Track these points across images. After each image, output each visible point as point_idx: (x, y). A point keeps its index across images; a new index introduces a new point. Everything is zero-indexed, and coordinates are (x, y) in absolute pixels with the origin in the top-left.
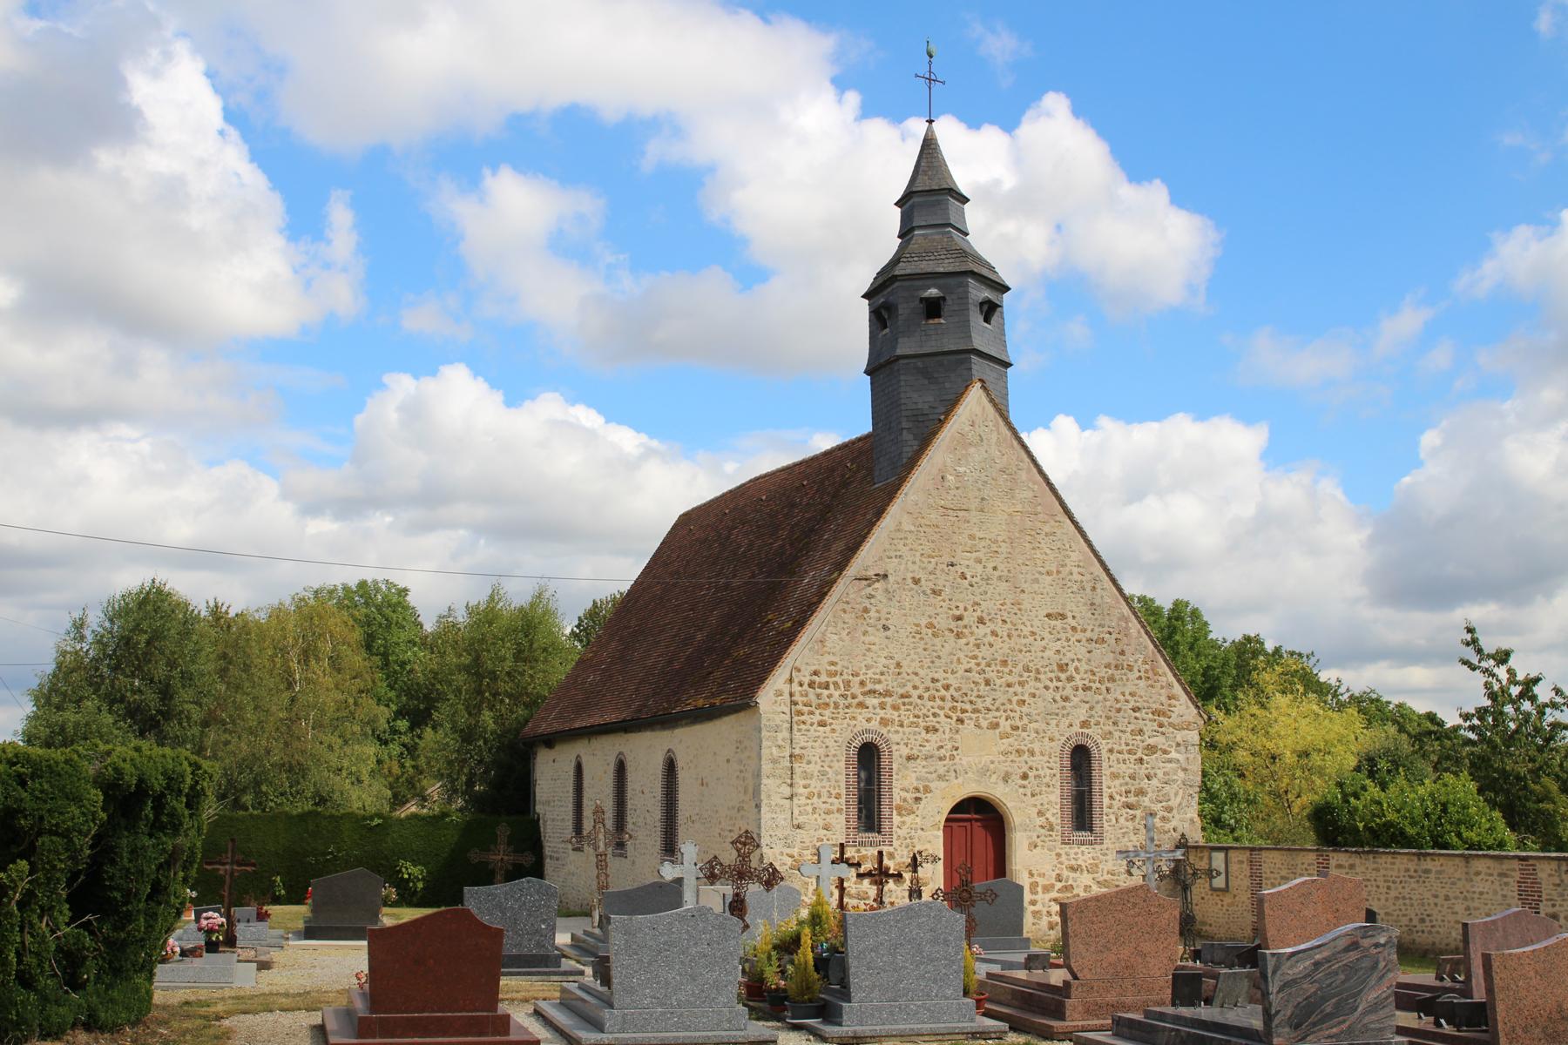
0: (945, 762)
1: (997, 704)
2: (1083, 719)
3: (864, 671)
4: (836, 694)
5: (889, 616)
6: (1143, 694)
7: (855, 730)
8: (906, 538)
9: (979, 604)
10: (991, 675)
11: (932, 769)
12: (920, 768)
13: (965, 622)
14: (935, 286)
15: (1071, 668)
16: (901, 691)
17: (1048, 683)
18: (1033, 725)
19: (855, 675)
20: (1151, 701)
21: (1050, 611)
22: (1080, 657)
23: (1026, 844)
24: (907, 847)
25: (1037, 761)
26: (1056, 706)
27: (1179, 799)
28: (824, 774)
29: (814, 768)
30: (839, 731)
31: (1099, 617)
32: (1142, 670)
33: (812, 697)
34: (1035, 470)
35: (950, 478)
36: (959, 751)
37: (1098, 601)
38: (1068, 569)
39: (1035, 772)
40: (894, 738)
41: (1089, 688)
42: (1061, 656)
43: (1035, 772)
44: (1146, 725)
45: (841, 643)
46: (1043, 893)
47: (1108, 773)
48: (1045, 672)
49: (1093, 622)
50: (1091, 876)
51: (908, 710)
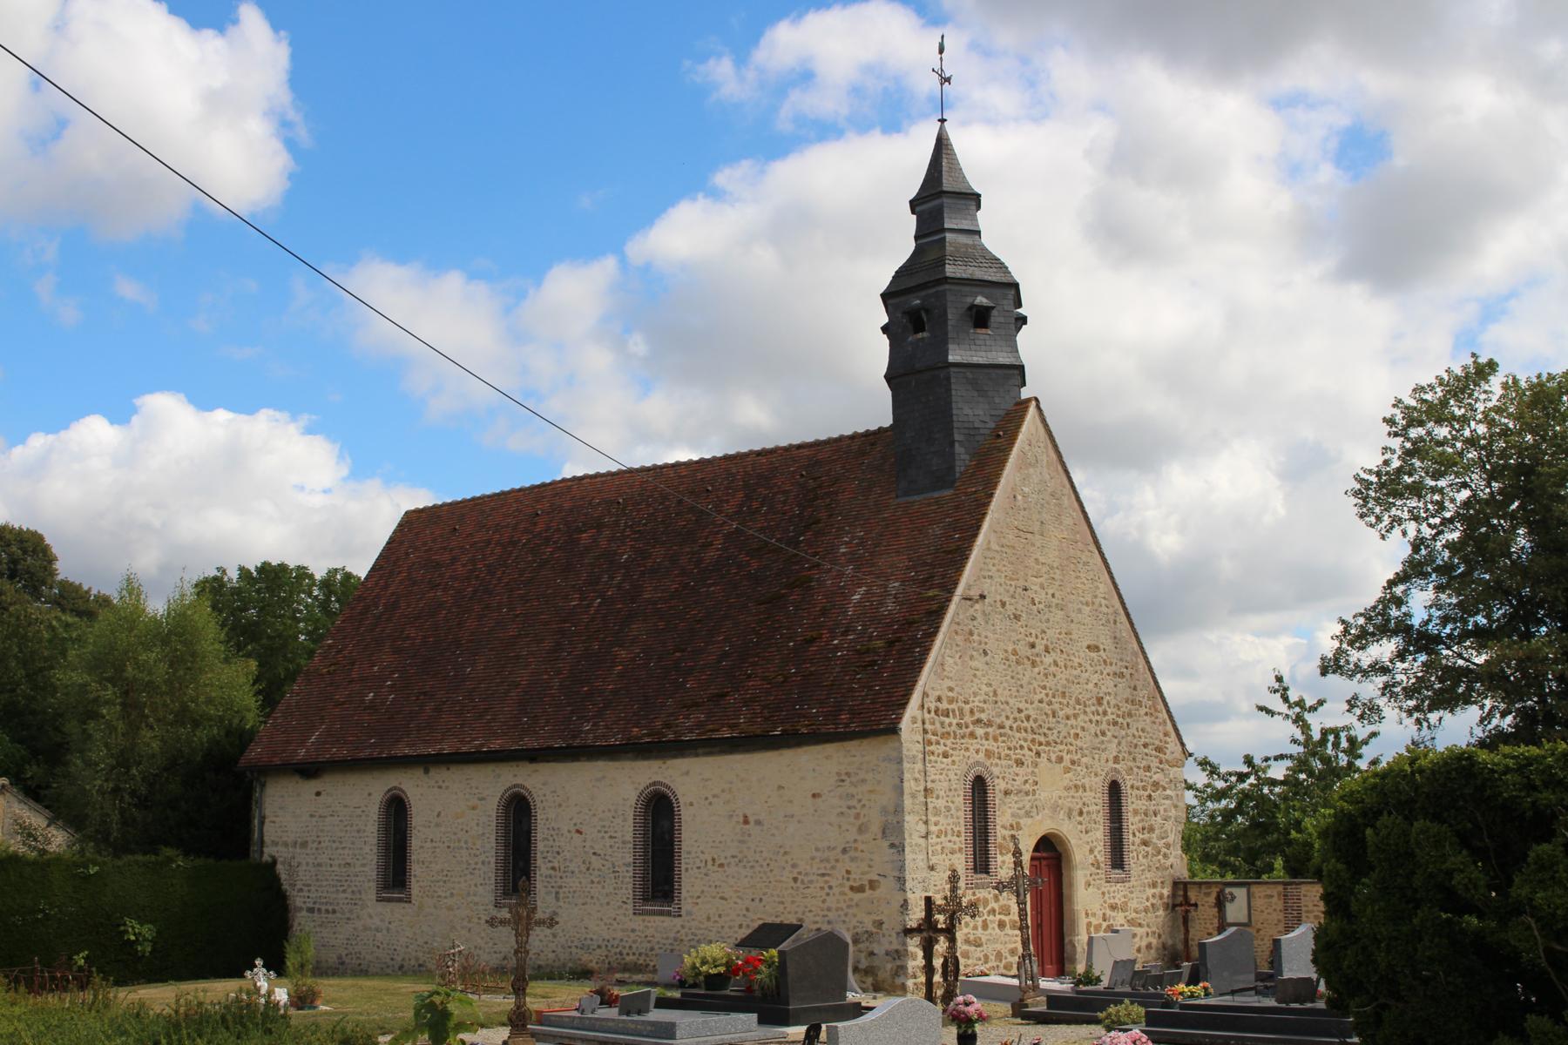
18: (1084, 760)
19: (966, 702)
34: (1073, 496)
40: (996, 771)
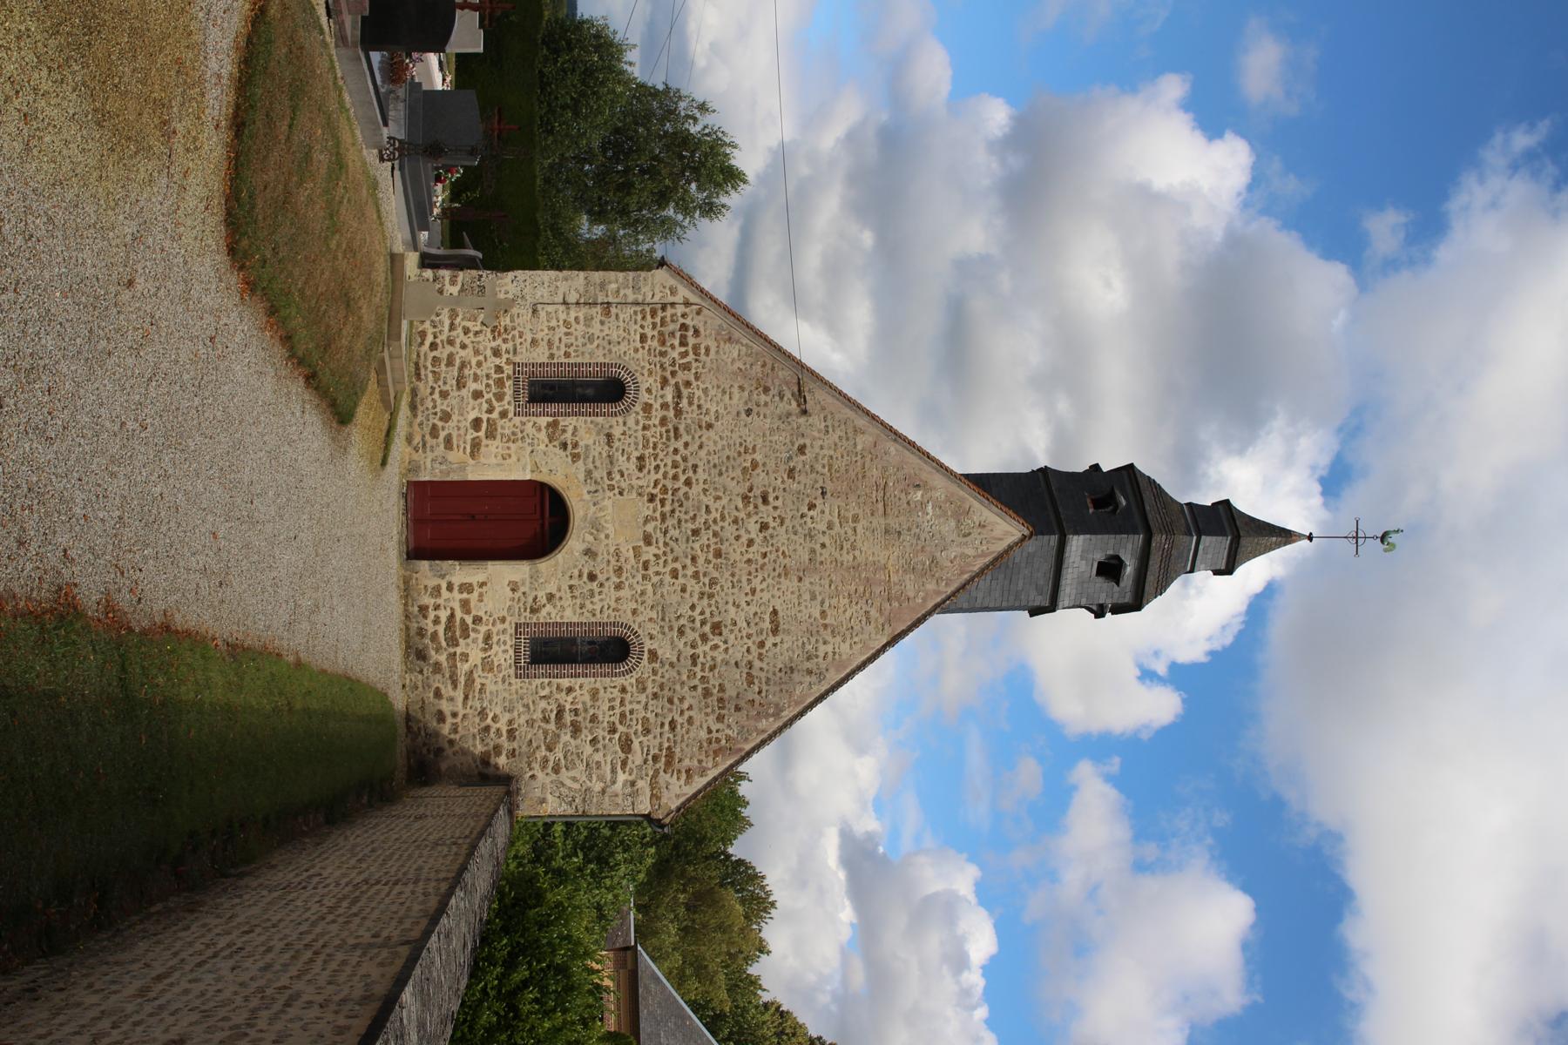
0: (605, 478)
1: (671, 543)
2: (660, 652)
3: (702, 386)
4: (675, 354)
5: (762, 417)
6: (692, 735)
7: (637, 374)
8: (847, 439)
9: (782, 523)
10: (705, 537)
11: (598, 463)
12: (599, 449)
13: (762, 508)
15: (716, 640)
16: (682, 428)
17: (698, 610)
18: (650, 589)
20: (684, 745)
21: (781, 614)
22: (730, 651)
23: (516, 578)
24: (514, 434)
25: (610, 594)
26: (673, 619)
27: (569, 783)
28: (591, 339)
29: (596, 328)
30: (637, 356)
31: (777, 679)
32: (719, 735)
33: (671, 327)
35: (919, 494)
36: (618, 496)
37: (796, 677)
38: (829, 638)
39: (597, 590)
40: (631, 421)
41: (694, 664)
42: (730, 627)
43: (597, 590)
44: (655, 737)
45: (730, 360)
46: (461, 600)
47: (598, 685)
48: (710, 606)
49: (772, 669)
50: (479, 662)
51: (661, 435)
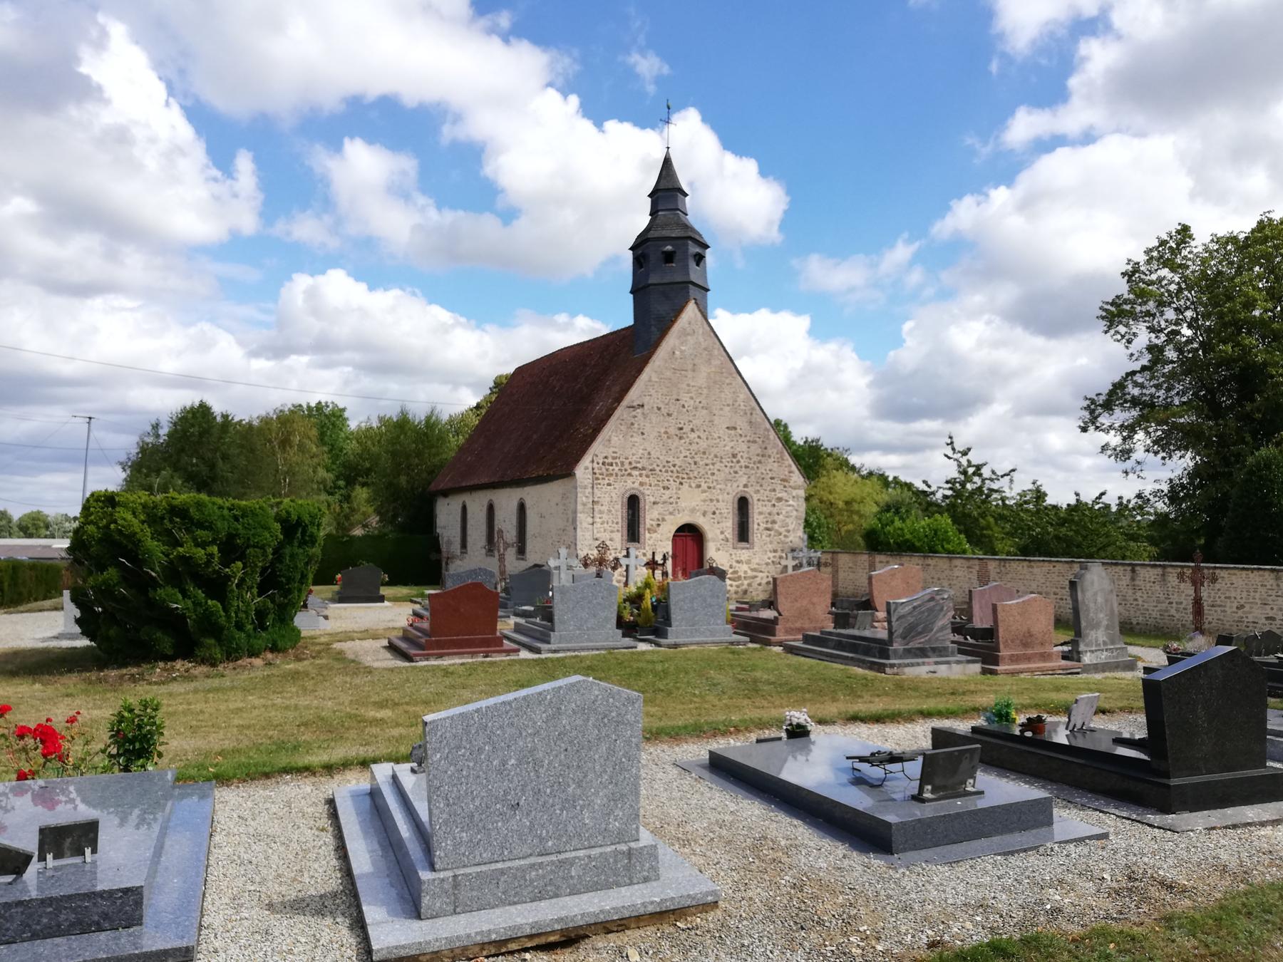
4: (617, 469)
10: (697, 459)
13: (684, 431)
14: (671, 245)
15: (739, 456)
16: (651, 468)
18: (719, 486)
19: (627, 458)
23: (714, 549)
25: (721, 505)
27: (793, 526)
28: (610, 511)
29: (605, 508)
33: (604, 470)
34: (722, 349)
37: (753, 420)
40: (647, 492)
